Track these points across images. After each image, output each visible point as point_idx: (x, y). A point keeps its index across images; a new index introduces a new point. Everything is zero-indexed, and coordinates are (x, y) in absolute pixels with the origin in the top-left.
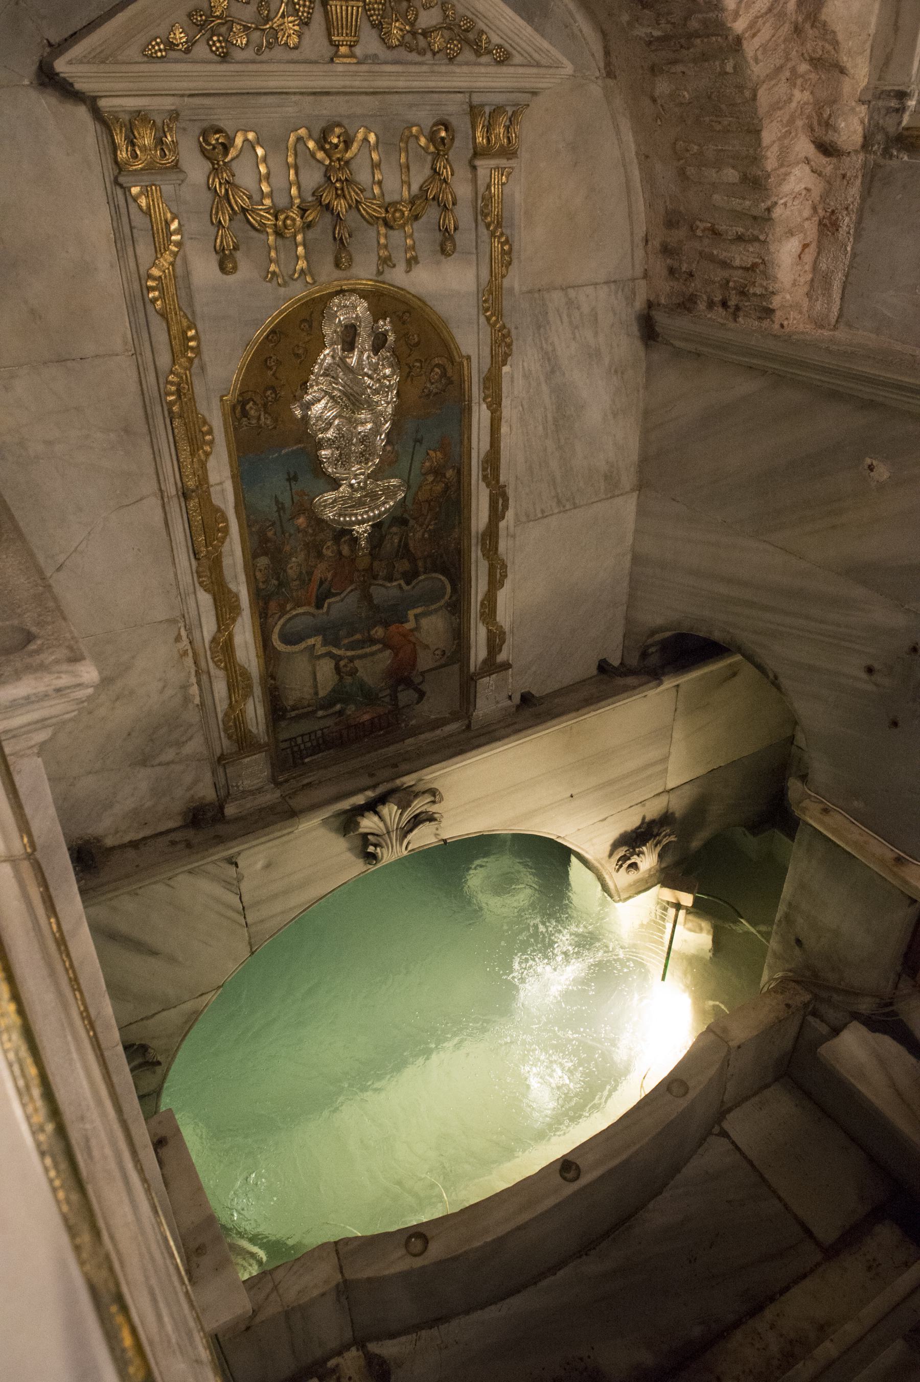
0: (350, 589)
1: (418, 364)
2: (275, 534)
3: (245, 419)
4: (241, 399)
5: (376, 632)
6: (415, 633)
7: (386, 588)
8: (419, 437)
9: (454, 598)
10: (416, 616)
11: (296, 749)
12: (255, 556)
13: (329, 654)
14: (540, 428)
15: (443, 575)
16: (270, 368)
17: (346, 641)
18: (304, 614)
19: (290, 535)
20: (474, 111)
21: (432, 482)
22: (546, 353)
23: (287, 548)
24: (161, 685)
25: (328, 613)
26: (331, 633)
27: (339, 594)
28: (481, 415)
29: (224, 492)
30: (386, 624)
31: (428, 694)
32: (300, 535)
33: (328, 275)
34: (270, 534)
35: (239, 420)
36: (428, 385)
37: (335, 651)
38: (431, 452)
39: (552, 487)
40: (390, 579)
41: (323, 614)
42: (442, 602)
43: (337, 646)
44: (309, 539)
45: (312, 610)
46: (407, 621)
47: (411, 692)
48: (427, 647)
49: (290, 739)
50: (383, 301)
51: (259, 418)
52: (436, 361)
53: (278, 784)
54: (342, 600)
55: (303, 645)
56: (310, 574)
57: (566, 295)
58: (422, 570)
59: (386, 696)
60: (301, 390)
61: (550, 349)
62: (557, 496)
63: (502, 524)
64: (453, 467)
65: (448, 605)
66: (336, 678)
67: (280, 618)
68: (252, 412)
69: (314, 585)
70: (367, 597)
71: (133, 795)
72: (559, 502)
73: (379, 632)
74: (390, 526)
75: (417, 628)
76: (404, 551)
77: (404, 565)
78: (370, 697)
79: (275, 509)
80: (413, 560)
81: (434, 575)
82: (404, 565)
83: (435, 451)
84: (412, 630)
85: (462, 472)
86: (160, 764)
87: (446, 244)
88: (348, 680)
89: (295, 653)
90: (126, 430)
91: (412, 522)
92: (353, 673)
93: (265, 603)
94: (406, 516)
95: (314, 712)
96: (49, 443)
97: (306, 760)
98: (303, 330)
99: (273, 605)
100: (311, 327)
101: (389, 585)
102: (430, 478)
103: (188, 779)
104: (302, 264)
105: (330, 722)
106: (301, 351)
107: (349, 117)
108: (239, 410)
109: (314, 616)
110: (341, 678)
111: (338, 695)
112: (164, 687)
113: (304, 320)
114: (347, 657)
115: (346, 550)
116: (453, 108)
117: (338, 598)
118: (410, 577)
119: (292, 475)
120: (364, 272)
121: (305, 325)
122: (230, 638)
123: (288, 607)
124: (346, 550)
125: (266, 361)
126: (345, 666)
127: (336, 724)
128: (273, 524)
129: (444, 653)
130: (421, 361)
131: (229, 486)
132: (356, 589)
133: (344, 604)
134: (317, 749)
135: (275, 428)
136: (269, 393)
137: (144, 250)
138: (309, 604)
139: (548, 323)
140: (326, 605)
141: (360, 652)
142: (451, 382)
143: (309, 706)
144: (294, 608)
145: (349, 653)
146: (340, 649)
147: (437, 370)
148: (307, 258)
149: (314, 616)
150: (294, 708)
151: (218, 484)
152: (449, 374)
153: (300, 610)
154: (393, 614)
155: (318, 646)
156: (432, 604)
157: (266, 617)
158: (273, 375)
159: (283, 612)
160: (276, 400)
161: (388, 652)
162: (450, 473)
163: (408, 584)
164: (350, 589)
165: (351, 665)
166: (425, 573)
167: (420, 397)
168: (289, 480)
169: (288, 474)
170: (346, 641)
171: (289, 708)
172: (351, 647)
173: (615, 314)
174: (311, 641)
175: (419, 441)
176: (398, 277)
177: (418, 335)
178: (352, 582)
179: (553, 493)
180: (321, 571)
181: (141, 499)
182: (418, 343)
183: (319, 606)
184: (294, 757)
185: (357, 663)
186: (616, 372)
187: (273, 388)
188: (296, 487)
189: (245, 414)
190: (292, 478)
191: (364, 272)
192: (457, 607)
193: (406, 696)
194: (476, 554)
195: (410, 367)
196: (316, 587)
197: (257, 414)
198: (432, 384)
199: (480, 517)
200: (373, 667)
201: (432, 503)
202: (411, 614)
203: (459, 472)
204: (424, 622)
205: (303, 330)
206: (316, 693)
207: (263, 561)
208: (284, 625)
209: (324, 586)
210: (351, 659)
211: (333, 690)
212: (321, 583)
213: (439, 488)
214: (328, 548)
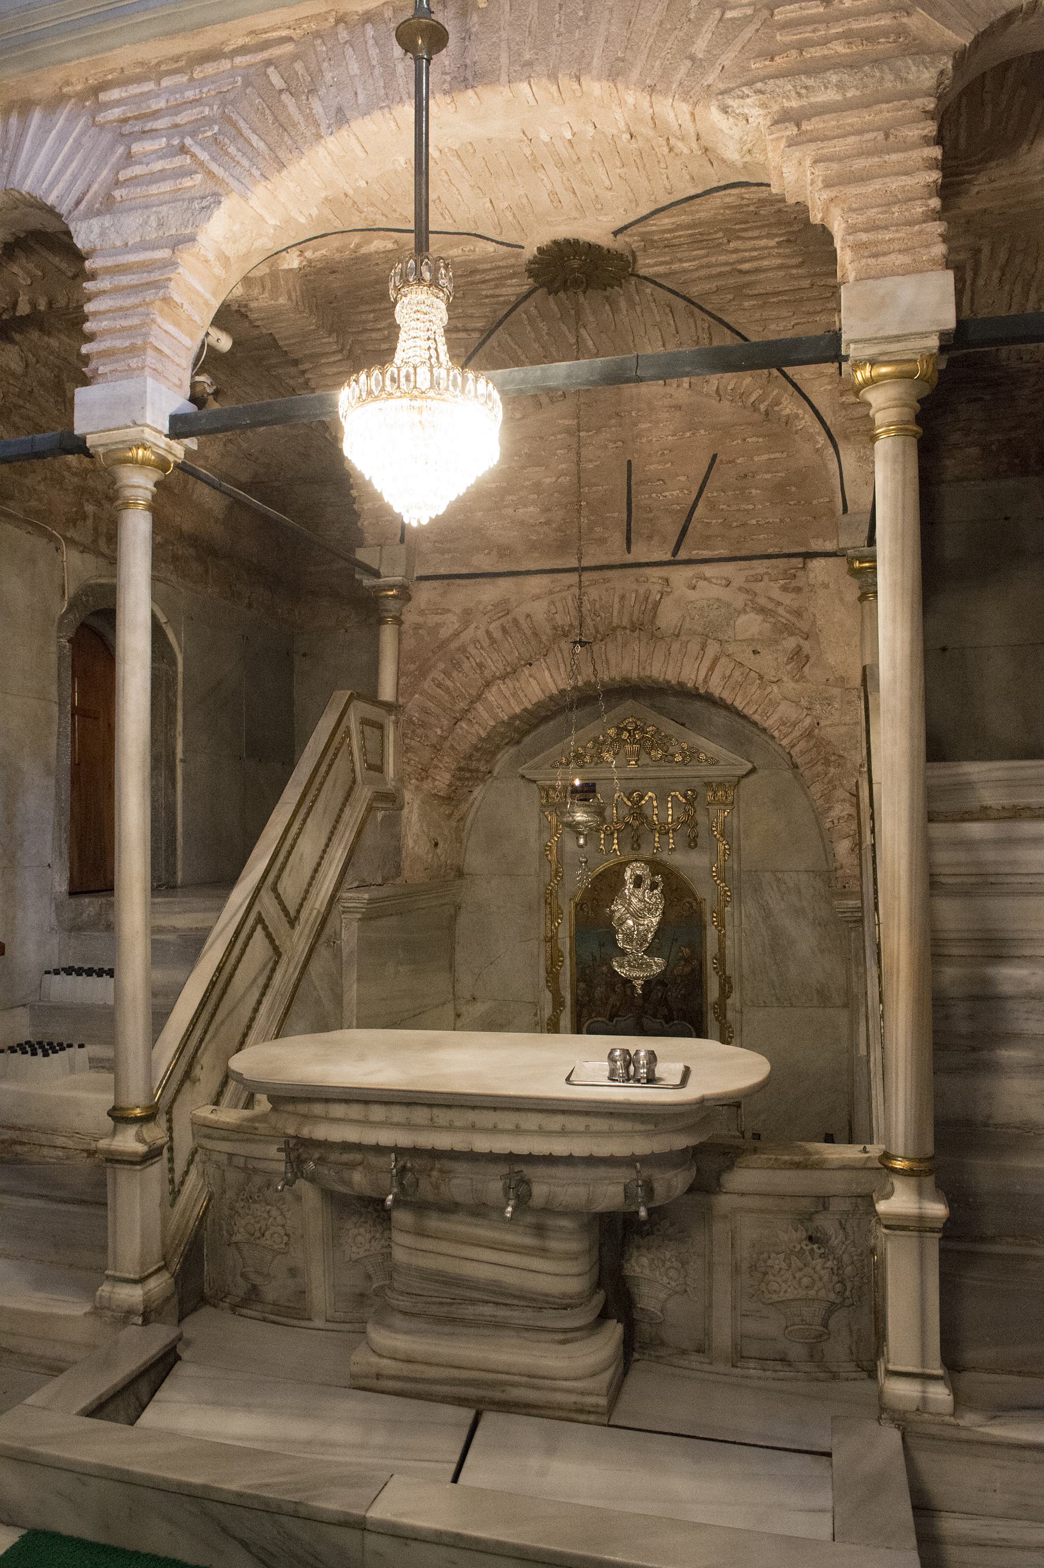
12: (578, 981)
14: (760, 949)
20: (708, 785)
22: (762, 906)
23: (595, 981)
25: (615, 1026)
28: (711, 933)
29: (565, 945)
34: (587, 972)
40: (655, 1016)
44: (609, 980)
50: (656, 866)
52: (687, 899)
56: (607, 1000)
63: (729, 1001)
69: (609, 1007)
72: (778, 999)
74: (656, 984)
85: (701, 964)
87: (692, 843)
96: (499, 908)
99: (585, 1011)
104: (616, 847)
108: (579, 906)
115: (629, 992)
116: (695, 783)
120: (646, 853)
122: (558, 1020)
124: (629, 992)
131: (568, 940)
137: (545, 836)
159: (590, 1017)
163: (667, 1023)
176: (665, 856)
180: (613, 999)
183: (611, 1019)
186: (820, 924)
189: (582, 909)
191: (646, 853)
194: (711, 1016)
199: (713, 991)
207: (582, 985)
212: (613, 1006)
213: (687, 969)
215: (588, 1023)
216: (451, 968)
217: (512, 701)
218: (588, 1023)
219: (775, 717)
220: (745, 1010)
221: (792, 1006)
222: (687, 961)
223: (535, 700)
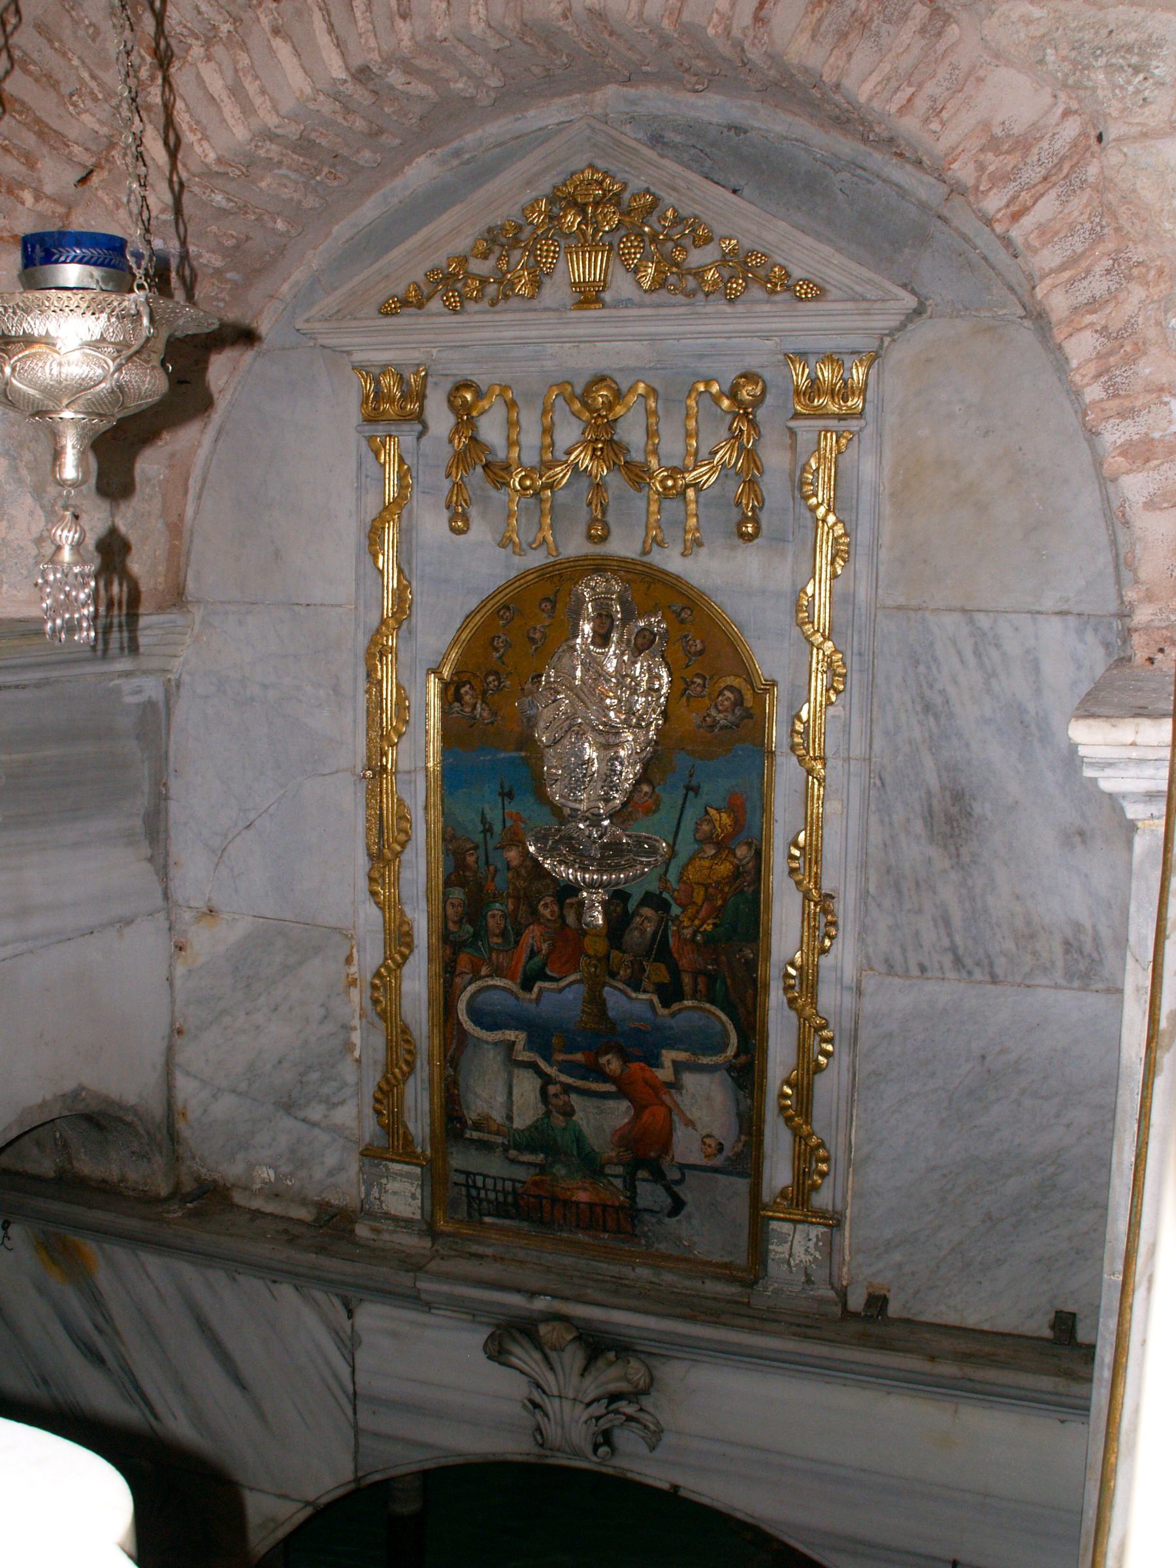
0: (572, 978)
1: (699, 681)
2: (477, 862)
3: (457, 704)
4: (455, 678)
5: (609, 1062)
6: (673, 1091)
7: (629, 998)
8: (694, 783)
9: (743, 1059)
10: (678, 1066)
11: (474, 1193)
12: (447, 883)
13: (533, 1066)
15: (722, 1010)
16: (497, 650)
17: (561, 1057)
18: (504, 989)
19: (496, 871)
21: (714, 857)
24: (322, 1011)
26: (541, 1036)
27: (557, 980)
30: (626, 1058)
31: (689, 1208)
32: (510, 875)
33: (575, 546)
34: (470, 860)
35: (450, 704)
36: (713, 712)
37: (542, 1064)
38: (712, 812)
39: (943, 932)
41: (530, 1001)
42: (719, 1059)
43: (547, 1059)
44: (521, 884)
45: (515, 988)
46: (659, 1065)
47: (660, 1190)
48: (690, 1123)
49: (468, 1174)
51: (474, 707)
53: (431, 1231)
54: (561, 990)
55: (496, 1036)
56: (519, 934)
57: (971, 622)
58: (687, 989)
59: (615, 1176)
60: (533, 683)
61: (938, 700)
62: (953, 949)
64: (749, 845)
65: (730, 1068)
66: (541, 1109)
67: (470, 983)
68: (467, 698)
70: (596, 1001)
71: (270, 1146)
73: (612, 1063)
75: (675, 1085)
76: (660, 950)
77: (658, 973)
78: (592, 1166)
79: (481, 828)
80: (675, 972)
81: (708, 1006)
82: (658, 973)
83: (718, 810)
84: (670, 1085)
85: (759, 856)
86: (304, 1120)
88: (559, 1120)
89: (487, 1042)
90: (336, 689)
91: (676, 910)
92: (568, 1112)
93: (454, 954)
94: (665, 895)
95: (506, 1149)
96: (265, 686)
97: (487, 1219)
98: (543, 610)
99: (464, 960)
100: (553, 607)
101: (634, 995)
102: (711, 851)
103: (331, 1160)
105: (521, 1174)
106: (537, 636)
107: (621, 370)
108: (451, 692)
109: (517, 998)
110: (548, 1114)
111: (538, 1140)
112: (325, 1017)
113: (547, 599)
114: (561, 1083)
117: (553, 985)
118: (670, 994)
119: (506, 790)
121: (547, 606)
123: (484, 971)
124: (571, 919)
125: (493, 639)
126: (556, 1095)
127: (535, 1183)
128: (476, 848)
129: (720, 1148)
130: (704, 679)
132: (580, 981)
133: (563, 997)
134: (500, 1210)
135: (492, 723)
136: (491, 678)
138: (513, 979)
139: (935, 659)
140: (536, 989)
141: (579, 1083)
142: (750, 716)
143: (498, 1133)
144: (489, 976)
145: (564, 1078)
146: (551, 1065)
147: (727, 694)
148: (552, 526)
149: (517, 998)
150: (477, 1126)
151: (409, 772)
152: (749, 703)
153: (498, 982)
154: (642, 1046)
155: (519, 1046)
156: (704, 1055)
157: (453, 973)
158: (500, 658)
159: (477, 977)
160: (499, 689)
161: (625, 1104)
162: (742, 851)
163: (666, 1004)
164: (572, 978)
165: (564, 1097)
166: (693, 997)
167: (700, 727)
168: (502, 795)
169: (502, 787)
170: (561, 1057)
171: (470, 1122)
172: (565, 1067)
173: (1079, 667)
174: (510, 1035)
175: (692, 789)
176: (671, 561)
177: (702, 642)
178: (576, 969)
179: (946, 942)
181: (337, 772)
182: (701, 653)
183: (527, 986)
184: (470, 1206)
185: (574, 1099)
187: (496, 673)
188: (512, 808)
189: (458, 698)
190: (507, 795)
192: (747, 1074)
193: (649, 1194)
195: (686, 683)
196: (524, 957)
197: (472, 701)
198: (719, 712)
200: (602, 1120)
201: (710, 890)
202: (669, 1056)
203: (758, 854)
204: (688, 1079)
205: (543, 610)
206: (510, 1118)
207: (457, 894)
208: (473, 996)
209: (536, 959)
210: (567, 1089)
211: (534, 1126)
212: (533, 954)
214: (546, 905)
215: (471, 989)
216: (155, 829)
217: (230, 109)
218: (471, 989)
219: (968, 120)
220: (869, 985)
221: (994, 980)
222: (723, 845)
223: (288, 104)
